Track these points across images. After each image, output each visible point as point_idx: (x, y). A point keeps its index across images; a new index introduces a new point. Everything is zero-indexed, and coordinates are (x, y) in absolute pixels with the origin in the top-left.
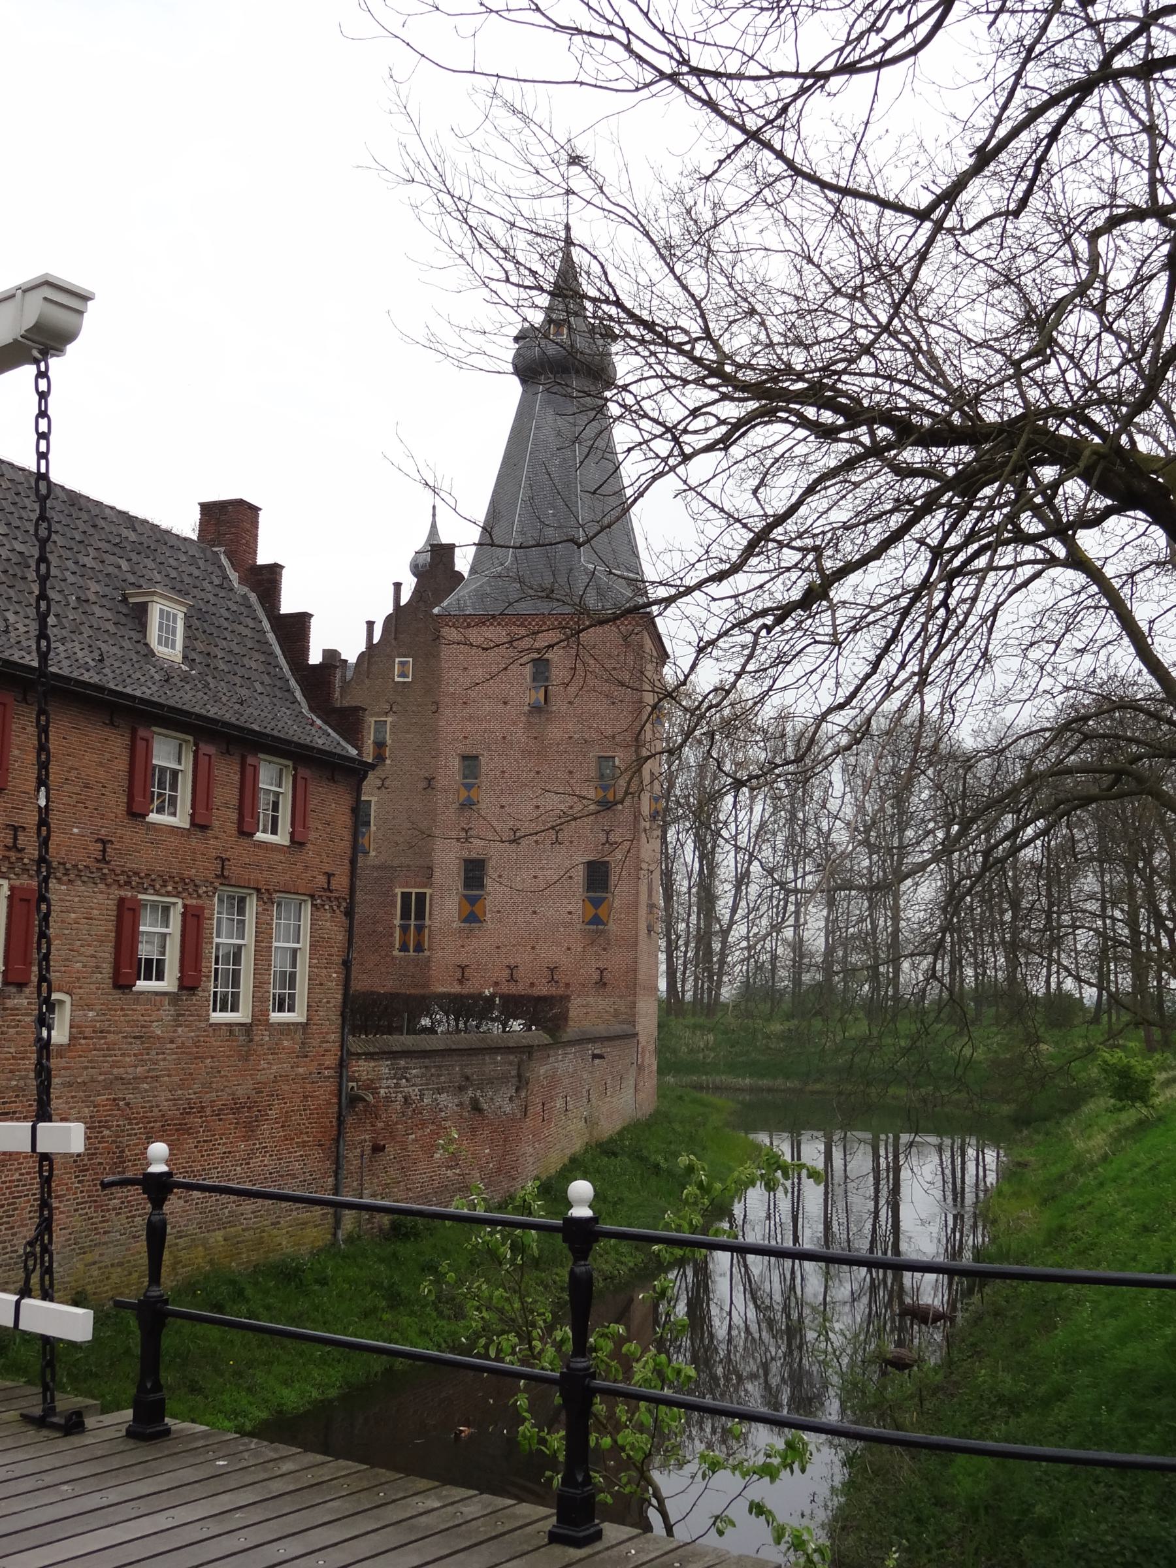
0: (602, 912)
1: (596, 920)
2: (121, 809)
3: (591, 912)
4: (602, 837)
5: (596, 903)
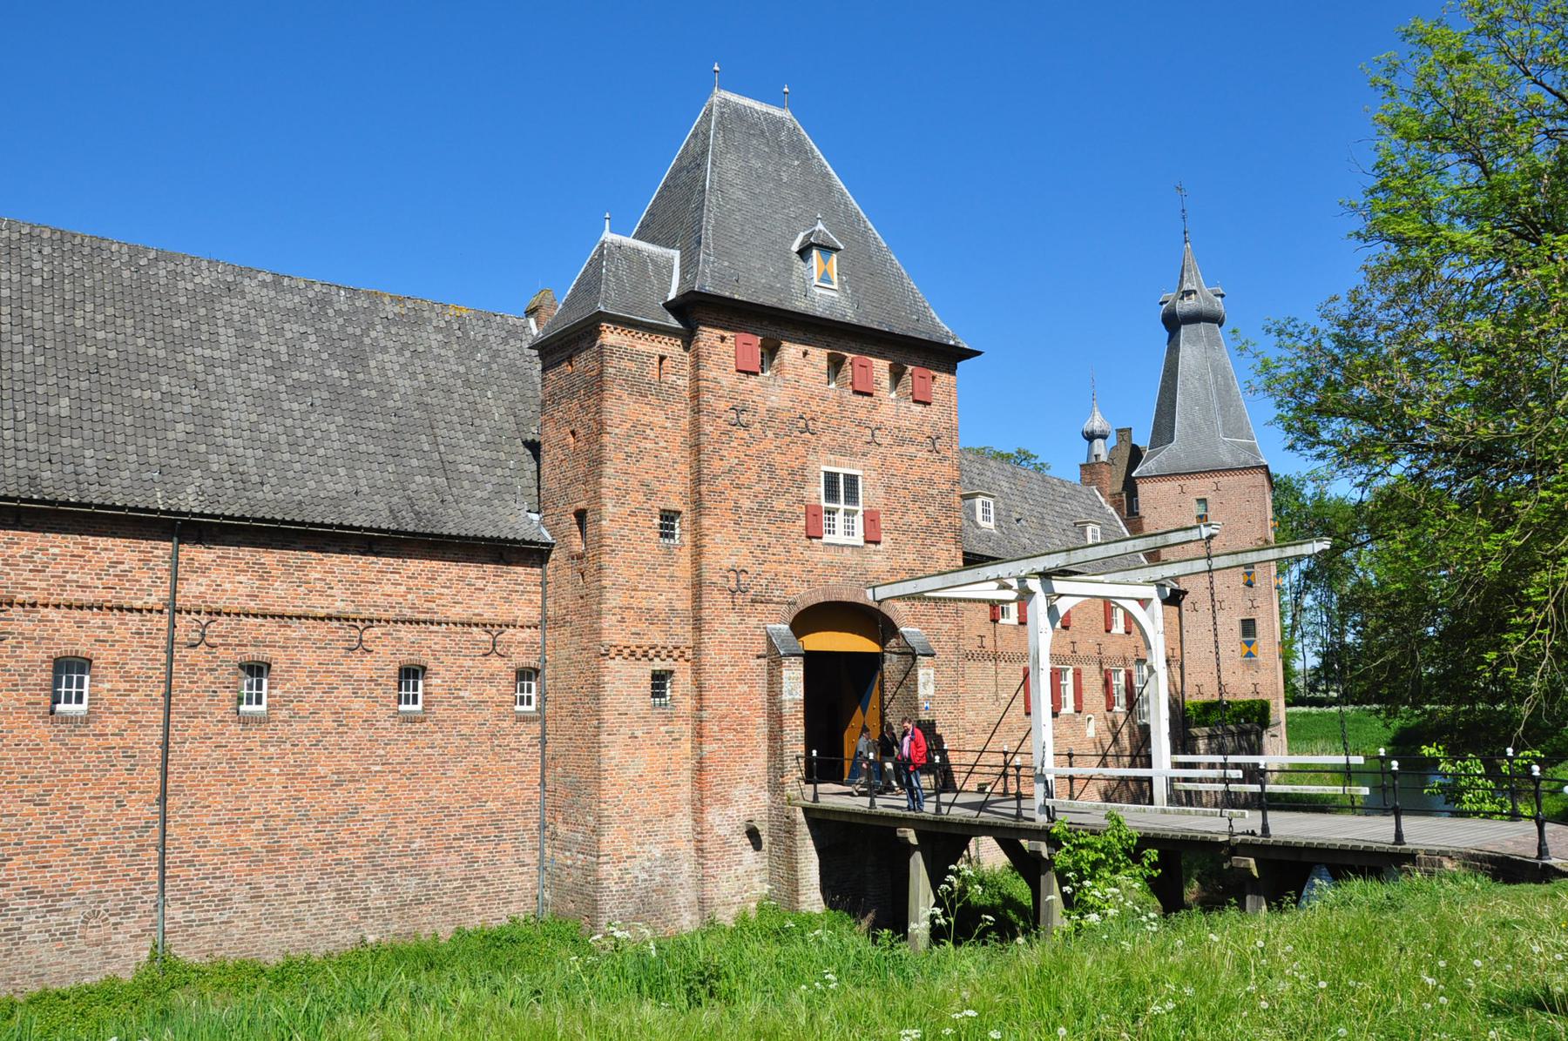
0: (1252, 649)
1: (1250, 655)
2: (1103, 629)
3: (1246, 649)
4: (1249, 604)
5: (1249, 644)
